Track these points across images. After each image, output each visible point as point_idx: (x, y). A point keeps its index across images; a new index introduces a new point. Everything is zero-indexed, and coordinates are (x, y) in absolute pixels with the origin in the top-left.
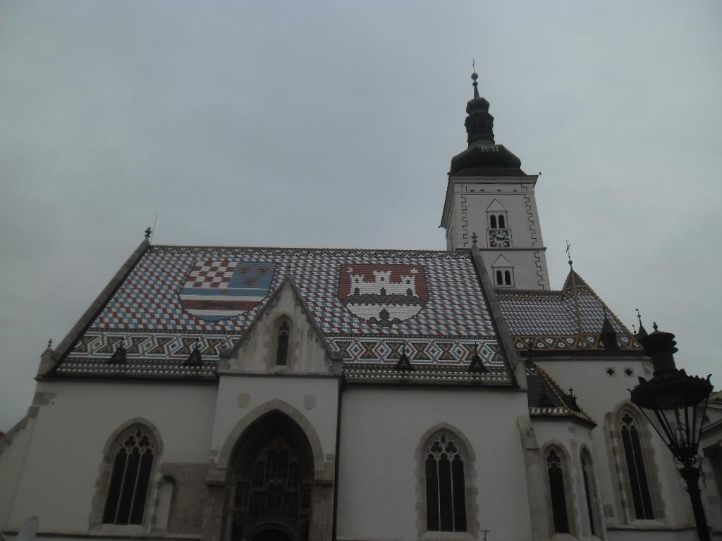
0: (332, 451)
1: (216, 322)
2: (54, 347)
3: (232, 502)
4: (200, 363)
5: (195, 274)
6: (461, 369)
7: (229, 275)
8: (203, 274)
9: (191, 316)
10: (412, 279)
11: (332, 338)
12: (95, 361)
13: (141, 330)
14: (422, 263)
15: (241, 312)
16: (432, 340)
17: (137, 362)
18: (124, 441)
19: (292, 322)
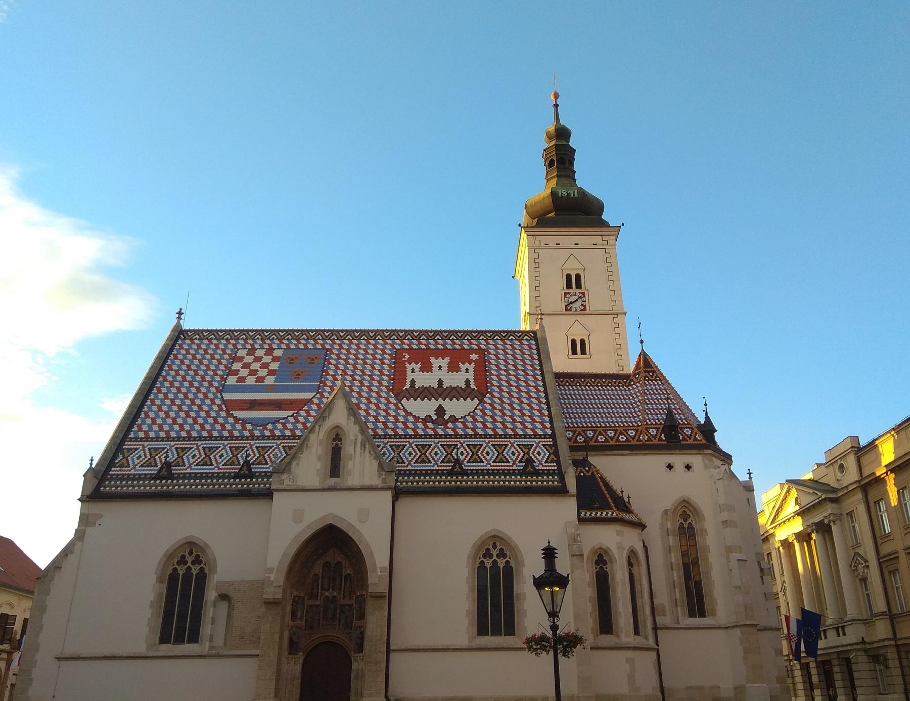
0: (386, 564)
1: (265, 426)
2: (93, 466)
3: (288, 617)
4: (251, 475)
5: (237, 366)
6: (514, 473)
7: (275, 366)
8: (246, 366)
9: (237, 420)
10: (471, 367)
11: (386, 441)
12: (140, 477)
13: (184, 439)
14: (484, 347)
15: (290, 413)
16: (487, 440)
17: (184, 476)
18: (176, 560)
19: (345, 434)
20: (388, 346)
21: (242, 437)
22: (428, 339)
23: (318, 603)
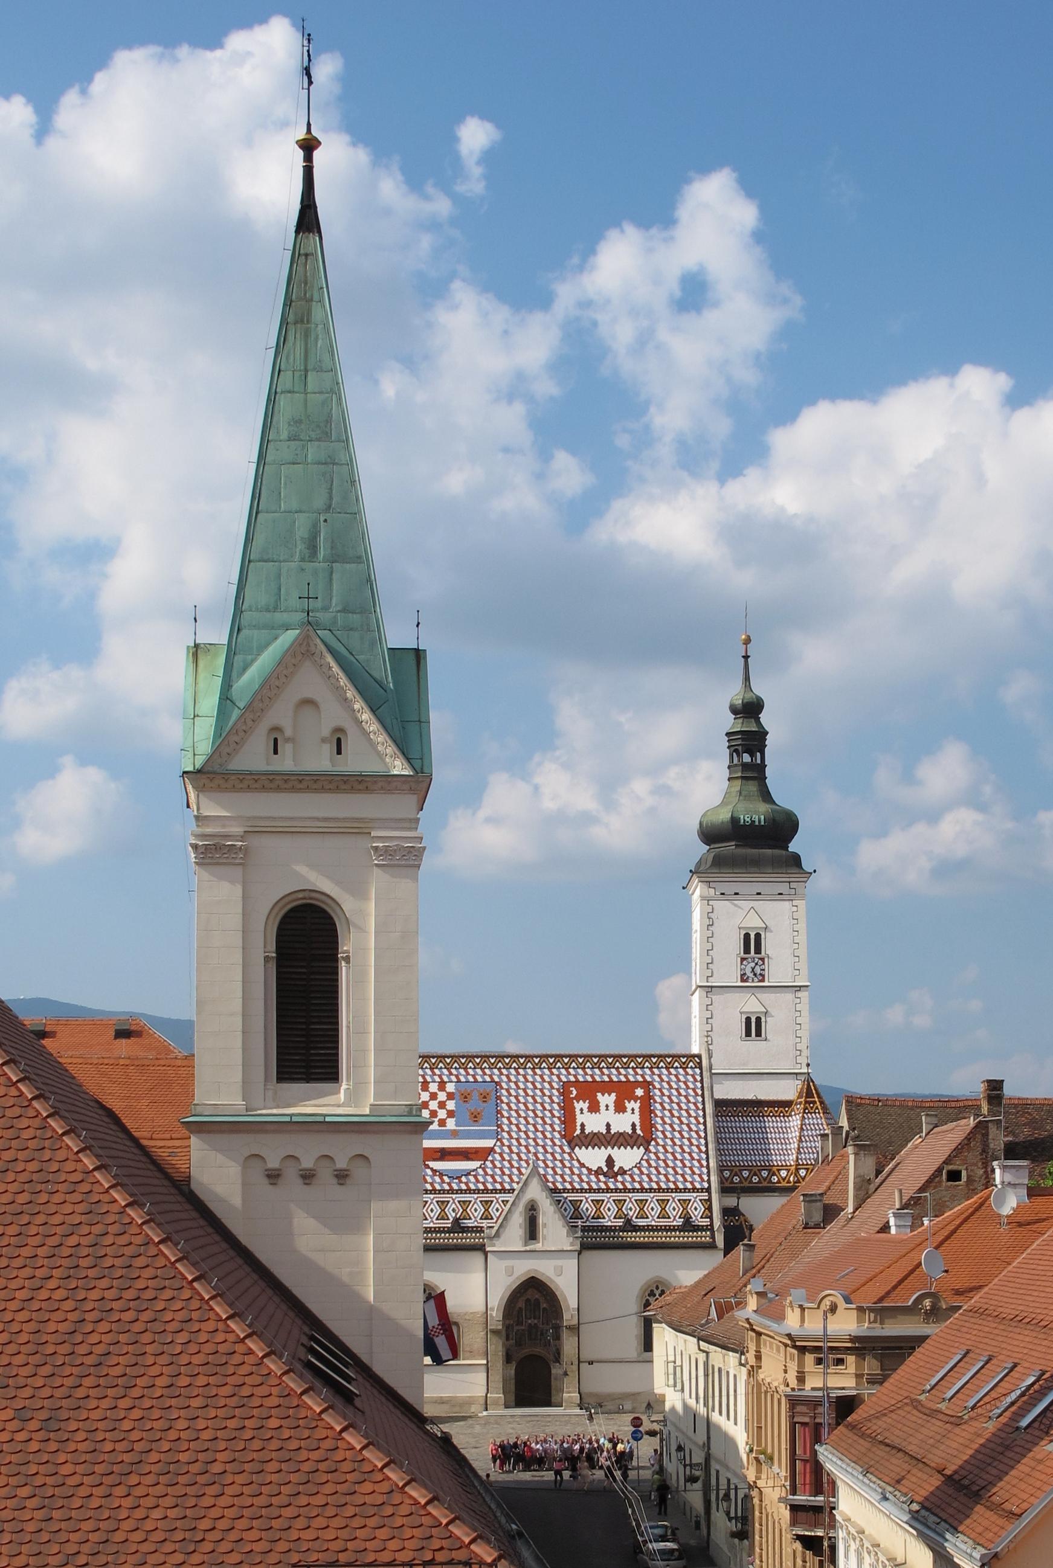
1: (459, 1178)
3: (504, 1338)
7: (451, 1105)
9: (434, 1171)
10: (637, 1106)
14: (649, 1079)
16: (652, 1195)
20: (555, 1078)
21: (443, 1191)
22: (593, 1068)
23: (523, 1328)
